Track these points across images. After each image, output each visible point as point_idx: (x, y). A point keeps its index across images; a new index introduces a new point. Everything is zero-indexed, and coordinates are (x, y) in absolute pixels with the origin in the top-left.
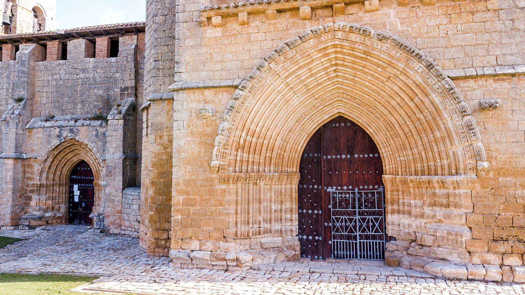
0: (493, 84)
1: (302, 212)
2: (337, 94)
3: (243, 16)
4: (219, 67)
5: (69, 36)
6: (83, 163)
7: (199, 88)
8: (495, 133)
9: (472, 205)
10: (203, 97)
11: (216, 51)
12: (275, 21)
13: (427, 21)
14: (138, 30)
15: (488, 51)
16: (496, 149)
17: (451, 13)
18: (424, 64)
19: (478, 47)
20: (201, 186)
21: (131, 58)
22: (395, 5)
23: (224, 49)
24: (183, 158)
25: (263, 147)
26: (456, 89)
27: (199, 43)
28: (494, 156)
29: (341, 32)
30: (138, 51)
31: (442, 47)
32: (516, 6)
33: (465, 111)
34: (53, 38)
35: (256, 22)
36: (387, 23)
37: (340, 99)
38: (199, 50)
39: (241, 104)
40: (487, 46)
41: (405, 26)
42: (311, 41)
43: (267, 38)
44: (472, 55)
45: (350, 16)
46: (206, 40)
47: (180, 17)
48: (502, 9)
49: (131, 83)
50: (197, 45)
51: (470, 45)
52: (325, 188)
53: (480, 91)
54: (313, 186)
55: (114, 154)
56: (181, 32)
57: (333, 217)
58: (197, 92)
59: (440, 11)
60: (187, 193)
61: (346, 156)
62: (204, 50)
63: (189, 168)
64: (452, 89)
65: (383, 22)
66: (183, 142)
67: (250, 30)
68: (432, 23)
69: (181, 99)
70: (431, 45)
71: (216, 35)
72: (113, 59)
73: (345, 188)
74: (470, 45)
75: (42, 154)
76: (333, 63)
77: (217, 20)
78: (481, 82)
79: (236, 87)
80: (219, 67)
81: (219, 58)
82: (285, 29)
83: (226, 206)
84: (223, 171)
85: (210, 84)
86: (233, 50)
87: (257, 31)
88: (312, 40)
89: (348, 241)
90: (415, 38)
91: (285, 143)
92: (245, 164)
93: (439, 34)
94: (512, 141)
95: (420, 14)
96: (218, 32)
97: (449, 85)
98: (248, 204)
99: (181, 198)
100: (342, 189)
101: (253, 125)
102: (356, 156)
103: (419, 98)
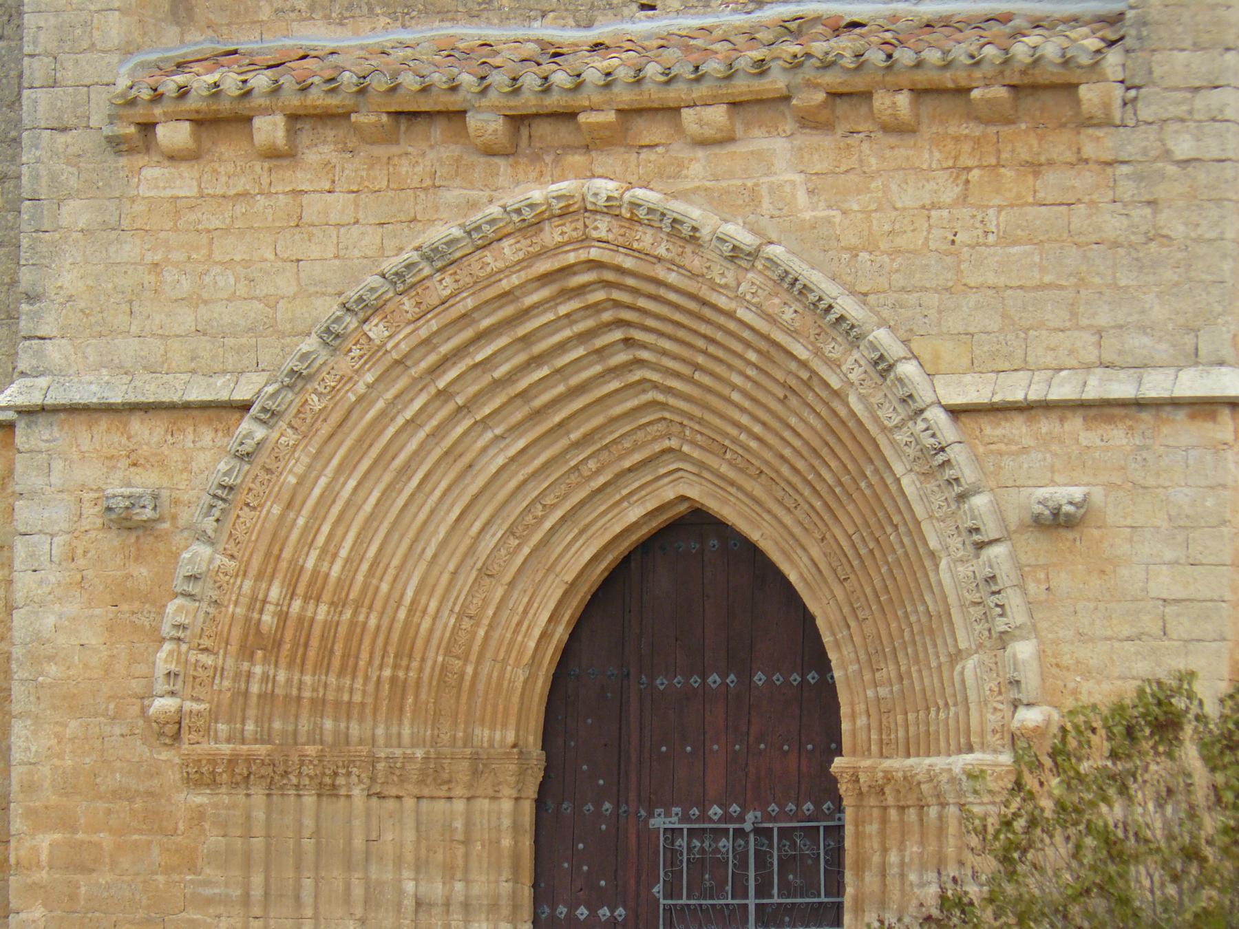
0: (1083, 434)
1: (553, 917)
2: (661, 426)
4: (186, 319)
7: (109, 409)
10: (124, 441)
11: (176, 256)
12: (394, 150)
13: (894, 187)
15: (1074, 314)
16: (1078, 662)
17: (970, 163)
18: (866, 353)
20: (116, 794)
23: (205, 251)
24: (51, 686)
26: (957, 454)
27: (113, 221)
28: (1071, 685)
29: (607, 219)
31: (936, 291)
32: (1167, 154)
33: (977, 530)
35: (320, 151)
36: (764, 191)
37: (674, 443)
38: (112, 249)
39: (263, 476)
41: (822, 204)
42: (505, 243)
43: (361, 215)
45: (645, 154)
46: (139, 207)
48: (1122, 162)
50: (105, 226)
51: (1021, 287)
52: (643, 813)
53: (1040, 456)
54: (598, 805)
56: (43, 172)
58: (104, 422)
59: (937, 155)
60: (67, 823)
61: (724, 676)
62: (130, 250)
63: (73, 724)
64: (942, 449)
65: (750, 184)
66: (51, 620)
67: (301, 179)
69: (44, 446)
70: (902, 283)
71: (176, 192)
73: (715, 811)
74: (1021, 287)
76: (607, 316)
77: (173, 134)
78: (1046, 425)
80: (186, 319)
81: (186, 285)
82: (428, 182)
83: (208, 871)
84: (194, 737)
85: (151, 392)
86: (238, 258)
87: (327, 186)
88: (511, 241)
90: (854, 252)
91: (466, 624)
93: (927, 239)
94: (1126, 633)
95: (873, 161)
96: (184, 182)
97: (933, 435)
98: (298, 868)
99: (45, 842)
100: (704, 817)
101: (314, 554)
102: (759, 678)
103: (876, 470)
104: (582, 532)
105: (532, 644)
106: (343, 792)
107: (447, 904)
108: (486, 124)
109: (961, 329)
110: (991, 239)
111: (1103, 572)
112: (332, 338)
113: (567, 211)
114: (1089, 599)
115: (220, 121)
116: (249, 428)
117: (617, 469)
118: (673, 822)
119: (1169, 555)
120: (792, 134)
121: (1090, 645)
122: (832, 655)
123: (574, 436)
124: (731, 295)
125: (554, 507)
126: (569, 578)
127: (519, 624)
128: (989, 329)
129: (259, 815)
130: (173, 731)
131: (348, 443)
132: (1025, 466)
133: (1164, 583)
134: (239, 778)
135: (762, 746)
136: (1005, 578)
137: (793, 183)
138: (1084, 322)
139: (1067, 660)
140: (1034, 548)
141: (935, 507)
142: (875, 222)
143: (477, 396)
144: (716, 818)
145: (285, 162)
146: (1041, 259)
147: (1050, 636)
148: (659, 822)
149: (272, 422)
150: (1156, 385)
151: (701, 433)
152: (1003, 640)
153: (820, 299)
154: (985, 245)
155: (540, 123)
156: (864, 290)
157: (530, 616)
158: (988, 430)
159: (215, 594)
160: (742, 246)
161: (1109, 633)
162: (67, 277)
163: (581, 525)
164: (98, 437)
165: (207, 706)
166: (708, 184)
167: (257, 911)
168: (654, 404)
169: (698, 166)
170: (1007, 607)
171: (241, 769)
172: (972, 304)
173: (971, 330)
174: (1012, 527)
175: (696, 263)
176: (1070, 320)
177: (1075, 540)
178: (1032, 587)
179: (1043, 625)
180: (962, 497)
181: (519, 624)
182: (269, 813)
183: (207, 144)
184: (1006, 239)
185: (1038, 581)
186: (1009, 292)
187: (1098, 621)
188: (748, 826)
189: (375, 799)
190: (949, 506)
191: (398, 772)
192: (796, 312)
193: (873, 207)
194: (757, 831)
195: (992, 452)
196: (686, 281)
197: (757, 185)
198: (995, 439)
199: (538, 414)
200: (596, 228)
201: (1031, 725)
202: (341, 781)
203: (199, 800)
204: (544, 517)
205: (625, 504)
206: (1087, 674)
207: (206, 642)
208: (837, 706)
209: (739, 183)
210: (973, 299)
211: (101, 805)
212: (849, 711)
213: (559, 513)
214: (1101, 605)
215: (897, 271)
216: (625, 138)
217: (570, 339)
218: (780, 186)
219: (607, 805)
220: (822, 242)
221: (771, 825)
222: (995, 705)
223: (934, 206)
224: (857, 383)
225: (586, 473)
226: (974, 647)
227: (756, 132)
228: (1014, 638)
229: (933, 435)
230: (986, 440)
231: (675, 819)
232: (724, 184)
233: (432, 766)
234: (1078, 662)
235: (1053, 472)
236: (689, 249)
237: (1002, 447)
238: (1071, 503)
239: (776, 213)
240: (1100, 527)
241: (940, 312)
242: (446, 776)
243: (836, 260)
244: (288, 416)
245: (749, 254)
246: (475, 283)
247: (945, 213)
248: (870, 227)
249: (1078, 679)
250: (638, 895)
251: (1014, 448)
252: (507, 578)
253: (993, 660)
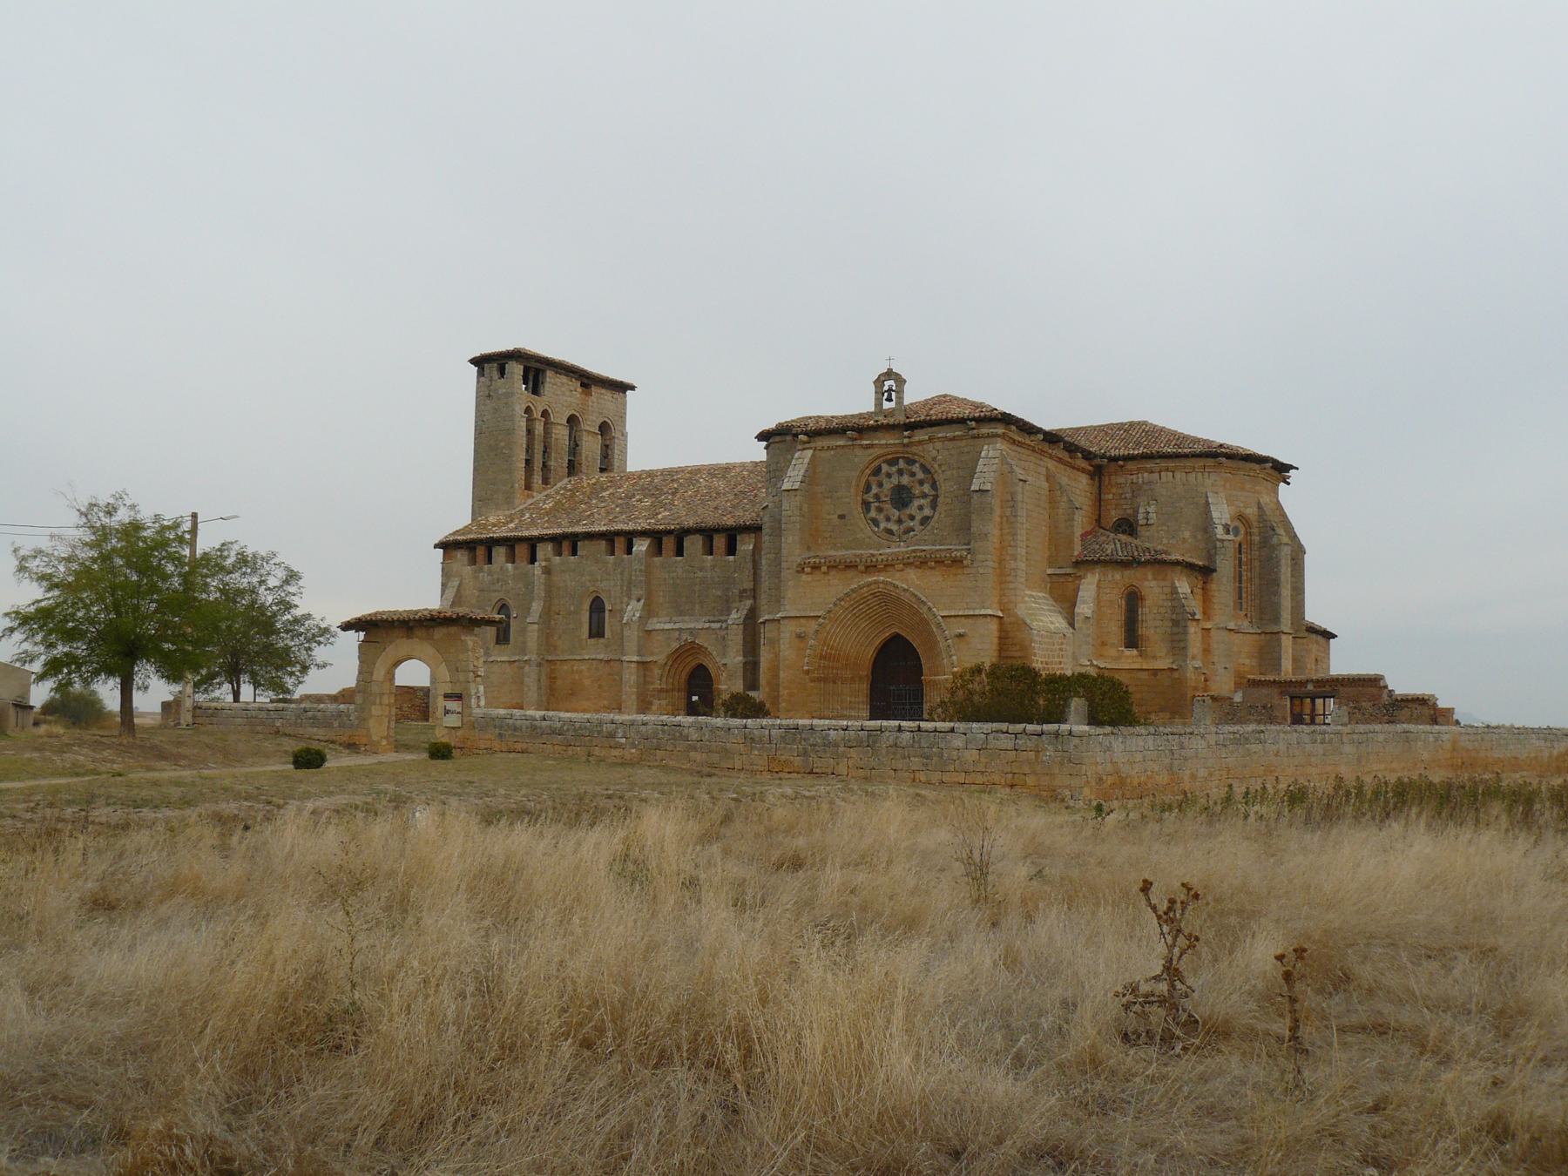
3: (824, 569)
5: (688, 531)
6: (701, 667)
14: (755, 529)
21: (749, 558)
30: (757, 550)
34: (670, 532)
35: (833, 573)
47: (784, 565)
49: (748, 585)
55: (735, 659)
72: (731, 558)
75: (660, 658)
77: (808, 570)
96: (809, 578)
108: (861, 568)
113: (876, 582)
115: (816, 567)
130: (808, 672)
150: (977, 612)
155: (871, 568)
162: (789, 594)
164: (794, 622)
169: (898, 575)
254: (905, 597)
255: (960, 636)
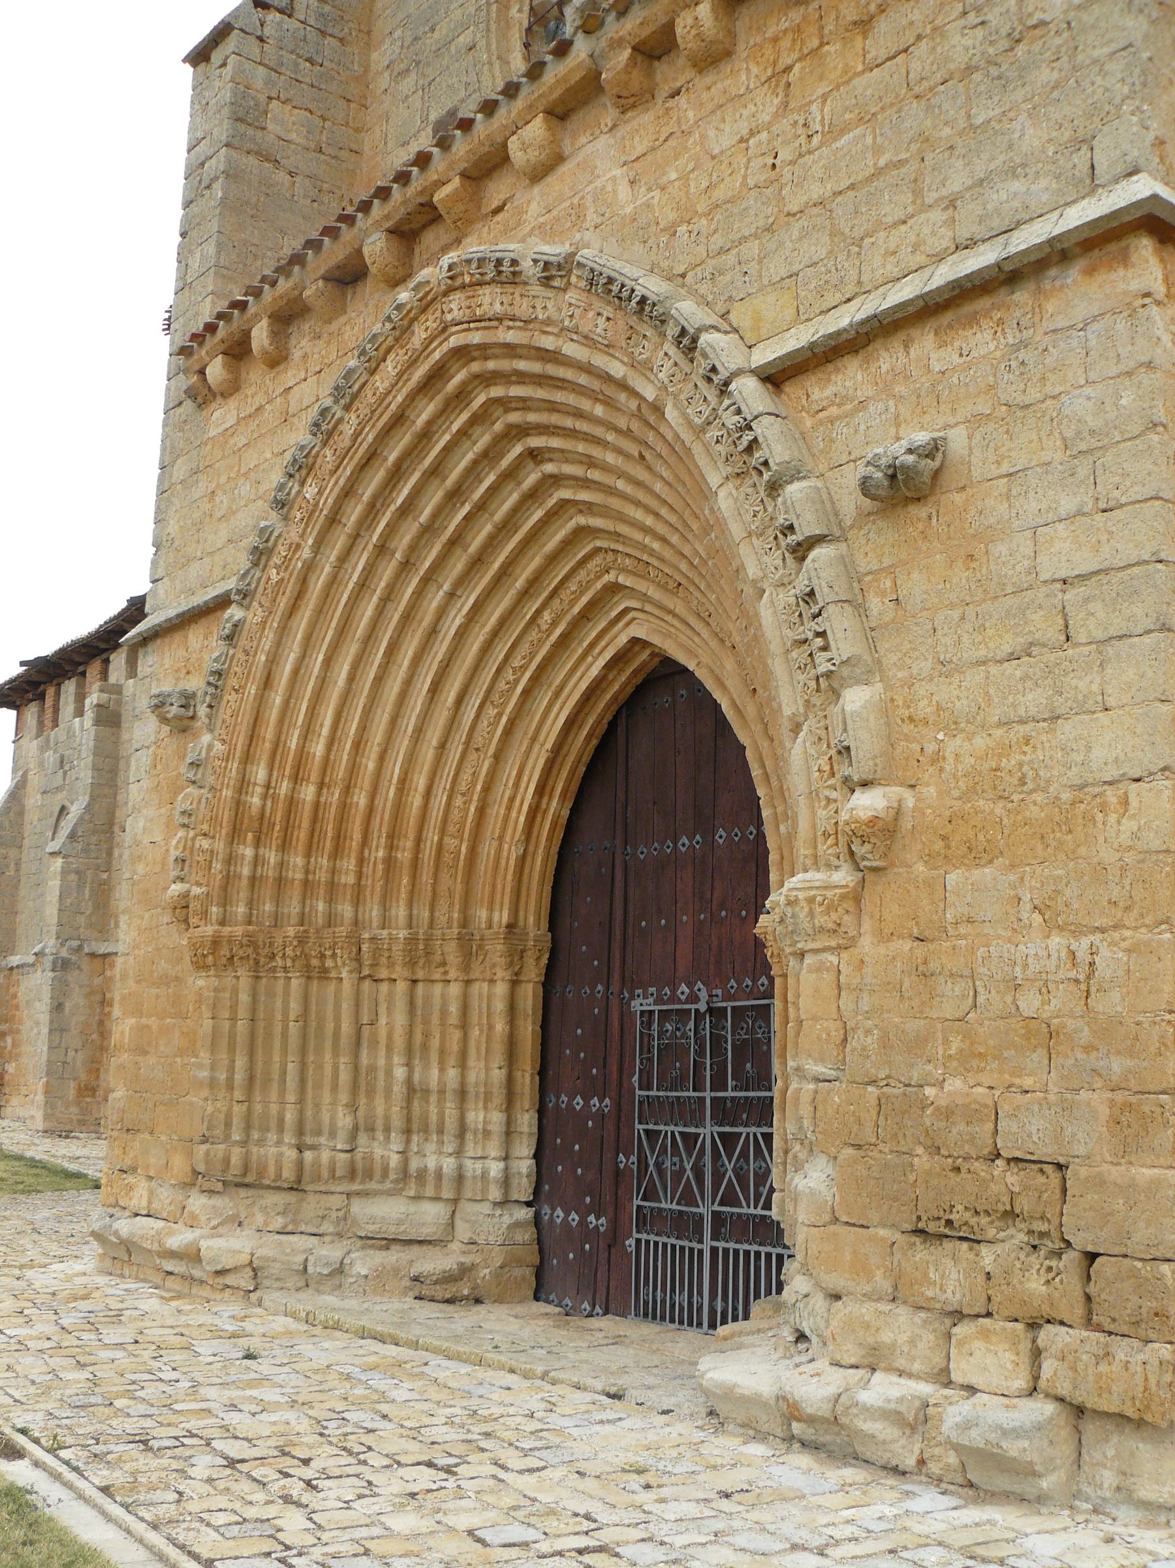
2: (598, 560)
8: (939, 618)
9: (837, 1036)
13: (711, 133)
16: (939, 708)
19: (878, 183)
22: (609, 116)
25: (376, 823)
26: (765, 429)
28: (931, 748)
31: (755, 236)
35: (301, 344)
36: (588, 202)
40: (914, 165)
44: (857, 234)
54: (593, 988)
57: (641, 1127)
59: (755, 70)
63: (147, 915)
68: (722, 137)
70: (720, 243)
74: (852, 187)
78: (888, 358)
79: (223, 602)
89: (679, 1243)
92: (267, 892)
93: (745, 177)
94: (1007, 649)
95: (691, 114)
100: (674, 999)
104: (557, 694)
105: (522, 819)
106: (333, 974)
107: (442, 1092)
109: (783, 273)
110: (816, 140)
111: (971, 557)
112: (281, 504)
114: (952, 606)
116: (235, 612)
117: (568, 617)
118: (648, 1004)
119: (1067, 505)
120: (614, 126)
121: (956, 679)
122: (760, 792)
123: (520, 584)
124: (556, 330)
125: (524, 668)
126: (549, 745)
127: (512, 800)
128: (815, 259)
129: (244, 998)
131: (308, 614)
132: (862, 427)
133: (1064, 553)
134: (224, 961)
135: (724, 913)
136: (826, 590)
137: (614, 179)
138: (930, 197)
139: (924, 708)
140: (874, 547)
141: (748, 517)
142: (692, 184)
143: (413, 548)
144: (683, 998)
145: (281, 367)
146: (875, 138)
147: (900, 675)
148: (637, 1005)
149: (245, 602)
151: (629, 556)
152: (830, 685)
153: (623, 286)
154: (810, 152)
156: (680, 269)
157: (522, 790)
158: (816, 394)
159: (211, 780)
160: (552, 259)
161: (982, 653)
163: (553, 688)
165: (204, 889)
166: (542, 220)
167: (238, 1095)
168: (580, 533)
169: (534, 203)
170: (829, 632)
171: (225, 951)
172: (796, 234)
173: (795, 268)
174: (848, 522)
175: (522, 308)
176: (914, 202)
177: (930, 517)
178: (875, 604)
179: (891, 659)
180: (774, 488)
181: (512, 800)
182: (254, 995)
183: (244, 375)
184: (834, 131)
185: (883, 594)
186: (839, 199)
187: (965, 638)
188: (702, 1007)
189: (367, 984)
190: (765, 510)
191: (386, 954)
192: (608, 319)
193: (690, 167)
194: (710, 1010)
195: (821, 422)
196: (521, 334)
197: (583, 198)
198: (825, 403)
199: (478, 561)
200: (451, 310)
201: (864, 815)
202: (329, 963)
203: (201, 983)
204: (517, 681)
205: (590, 659)
206: (953, 728)
207: (205, 827)
208: (767, 852)
209: (567, 204)
210: (796, 227)
211: (154, 991)
212: (777, 857)
213: (528, 675)
214: (970, 611)
215: (715, 231)
216: (480, 208)
217: (475, 462)
218: (604, 188)
219: (600, 987)
220: (641, 232)
221: (724, 1004)
222: (827, 792)
223: (752, 133)
224: (666, 381)
225: (544, 627)
226: (802, 710)
227: (583, 140)
228: (845, 683)
229: (739, 412)
230: (816, 407)
231: (651, 1000)
232: (555, 213)
233: (421, 947)
234: (939, 708)
235: (898, 426)
236: (518, 290)
237: (834, 411)
238: (910, 451)
239: (599, 221)
240: (964, 488)
241: (760, 262)
242: (437, 958)
243: (655, 249)
244: (258, 596)
245: (560, 267)
246: (373, 412)
247: (764, 135)
248: (687, 193)
249: (940, 736)
250: (620, 1085)
251: (849, 407)
252: (492, 751)
253: (822, 724)
254: (571, 325)
255: (902, 489)
